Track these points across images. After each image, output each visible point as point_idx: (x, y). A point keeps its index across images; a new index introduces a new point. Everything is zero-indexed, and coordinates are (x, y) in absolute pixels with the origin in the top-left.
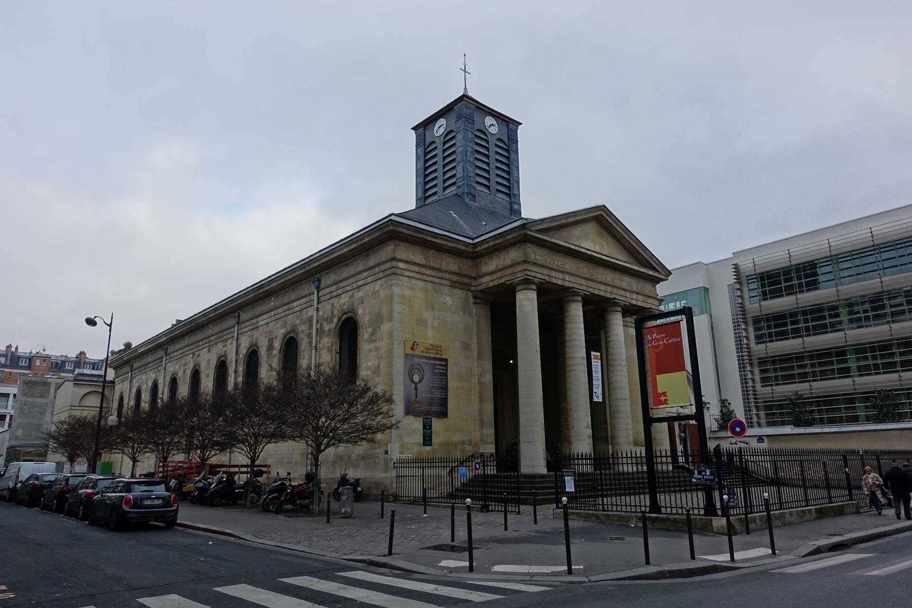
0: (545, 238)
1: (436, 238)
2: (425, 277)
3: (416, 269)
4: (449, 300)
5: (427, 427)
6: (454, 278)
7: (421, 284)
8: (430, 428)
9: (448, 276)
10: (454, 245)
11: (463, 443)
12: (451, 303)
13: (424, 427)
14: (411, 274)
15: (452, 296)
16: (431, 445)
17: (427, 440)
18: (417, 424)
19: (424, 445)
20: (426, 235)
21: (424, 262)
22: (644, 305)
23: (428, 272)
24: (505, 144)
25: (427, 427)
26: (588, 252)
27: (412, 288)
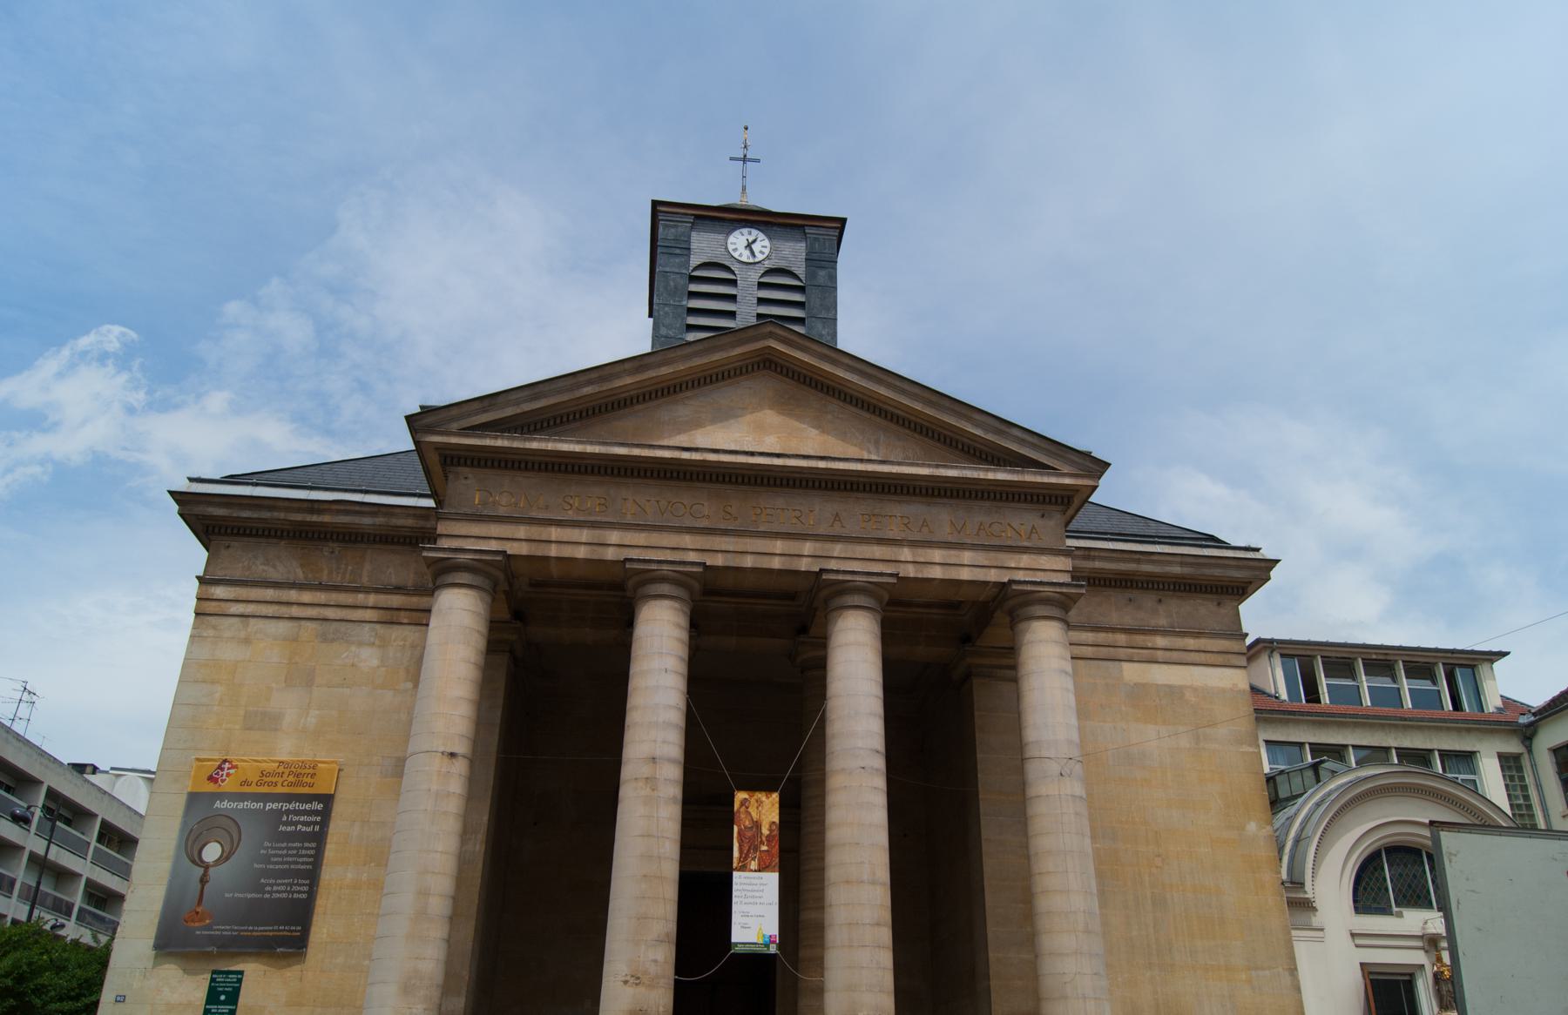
0: (535, 445)
1: (320, 512)
2: (295, 611)
3: (270, 594)
4: (369, 658)
6: (396, 600)
7: (282, 627)
8: (233, 997)
9: (372, 599)
10: (380, 520)
12: (375, 662)
15: (383, 644)
20: (287, 510)
21: (300, 575)
22: (993, 576)
23: (307, 597)
24: (795, 276)
26: (686, 455)
27: (247, 641)
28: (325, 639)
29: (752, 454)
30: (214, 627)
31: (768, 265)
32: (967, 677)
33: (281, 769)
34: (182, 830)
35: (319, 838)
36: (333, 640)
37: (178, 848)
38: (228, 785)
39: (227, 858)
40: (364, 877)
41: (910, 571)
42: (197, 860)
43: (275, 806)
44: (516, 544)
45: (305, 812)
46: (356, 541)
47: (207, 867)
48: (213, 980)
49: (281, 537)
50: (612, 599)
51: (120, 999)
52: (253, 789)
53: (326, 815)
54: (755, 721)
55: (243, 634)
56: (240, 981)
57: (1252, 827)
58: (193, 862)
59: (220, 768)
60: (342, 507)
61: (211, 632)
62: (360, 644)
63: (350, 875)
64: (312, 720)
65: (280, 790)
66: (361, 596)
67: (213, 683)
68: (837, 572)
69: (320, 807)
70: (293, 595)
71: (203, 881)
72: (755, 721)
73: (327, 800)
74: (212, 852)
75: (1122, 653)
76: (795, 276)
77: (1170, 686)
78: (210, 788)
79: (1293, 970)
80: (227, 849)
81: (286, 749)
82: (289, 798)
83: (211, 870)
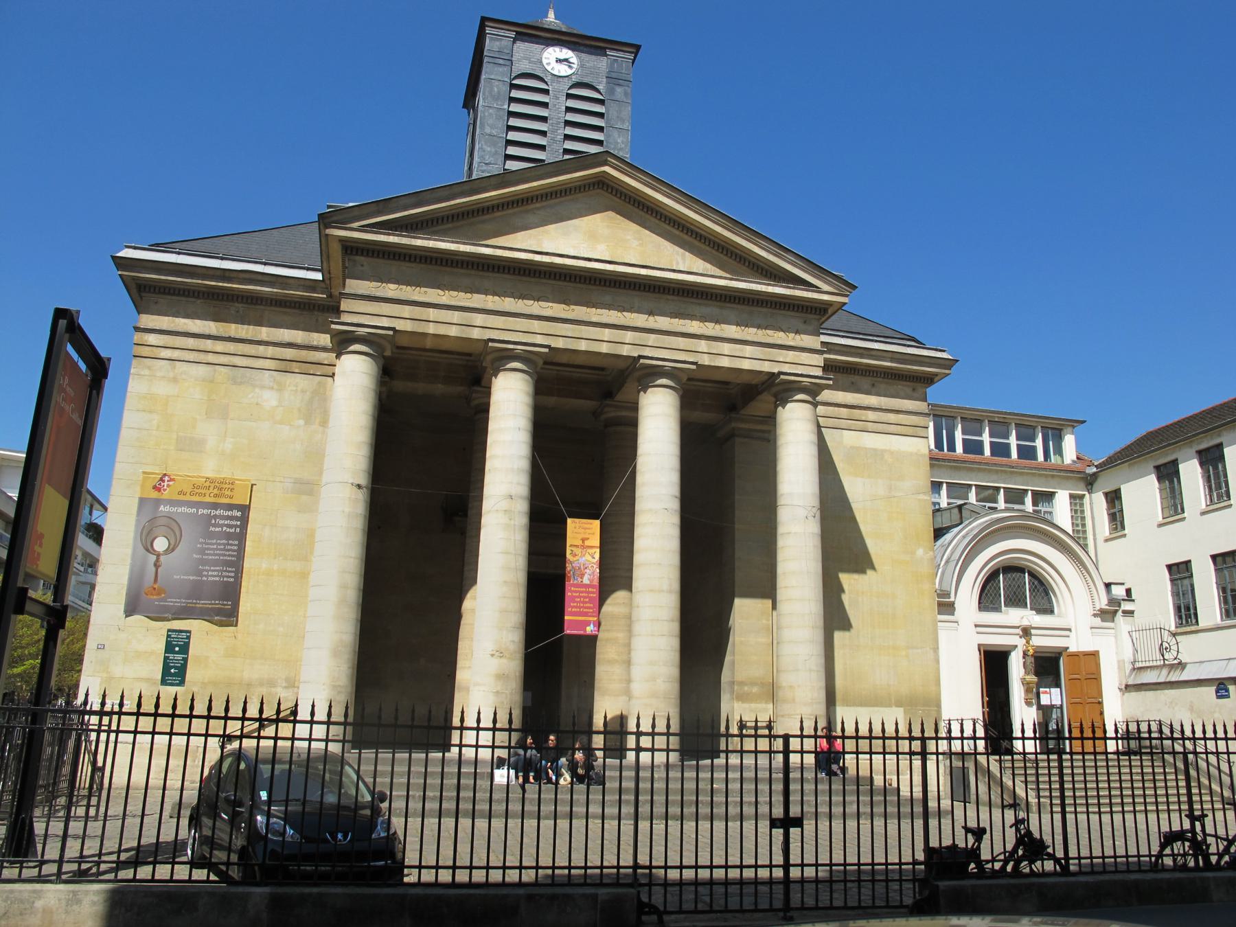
2: (211, 358)
3: (191, 342)
4: (269, 399)
5: (177, 647)
7: (202, 369)
8: (185, 649)
11: (272, 683)
12: (274, 403)
13: (169, 648)
14: (176, 354)
15: (281, 388)
16: (182, 683)
17: (174, 672)
18: (149, 638)
19: (164, 682)
22: (767, 367)
23: (220, 346)
24: (598, 91)
25: (177, 647)
26: (538, 258)
27: (175, 380)
28: (235, 382)
29: (589, 260)
30: (149, 368)
31: (575, 79)
32: (732, 435)
33: (207, 484)
34: (137, 526)
35: (242, 537)
36: (241, 383)
37: (135, 538)
38: (166, 494)
39: (173, 550)
40: (275, 567)
41: (706, 360)
42: (149, 549)
43: (205, 512)
44: (402, 321)
45: (228, 518)
46: (256, 304)
47: (158, 555)
48: (168, 636)
49: (198, 297)
50: (471, 369)
51: (101, 647)
52: (188, 498)
53: (244, 520)
54: (581, 462)
55: (171, 375)
56: (189, 638)
57: (920, 552)
58: (148, 550)
59: (162, 480)
60: (247, 276)
61: (146, 372)
62: (262, 387)
63: (264, 566)
64: (228, 446)
65: (207, 499)
66: (262, 348)
67: (150, 412)
68: (652, 358)
69: (239, 514)
70: (209, 345)
71: (157, 565)
72: (581, 462)
73: (245, 509)
74: (160, 544)
75: (844, 423)
76: (598, 91)
77: (875, 450)
78: (154, 495)
79: (936, 649)
80: (172, 542)
81: (210, 468)
82: (215, 506)
83: (162, 558)
